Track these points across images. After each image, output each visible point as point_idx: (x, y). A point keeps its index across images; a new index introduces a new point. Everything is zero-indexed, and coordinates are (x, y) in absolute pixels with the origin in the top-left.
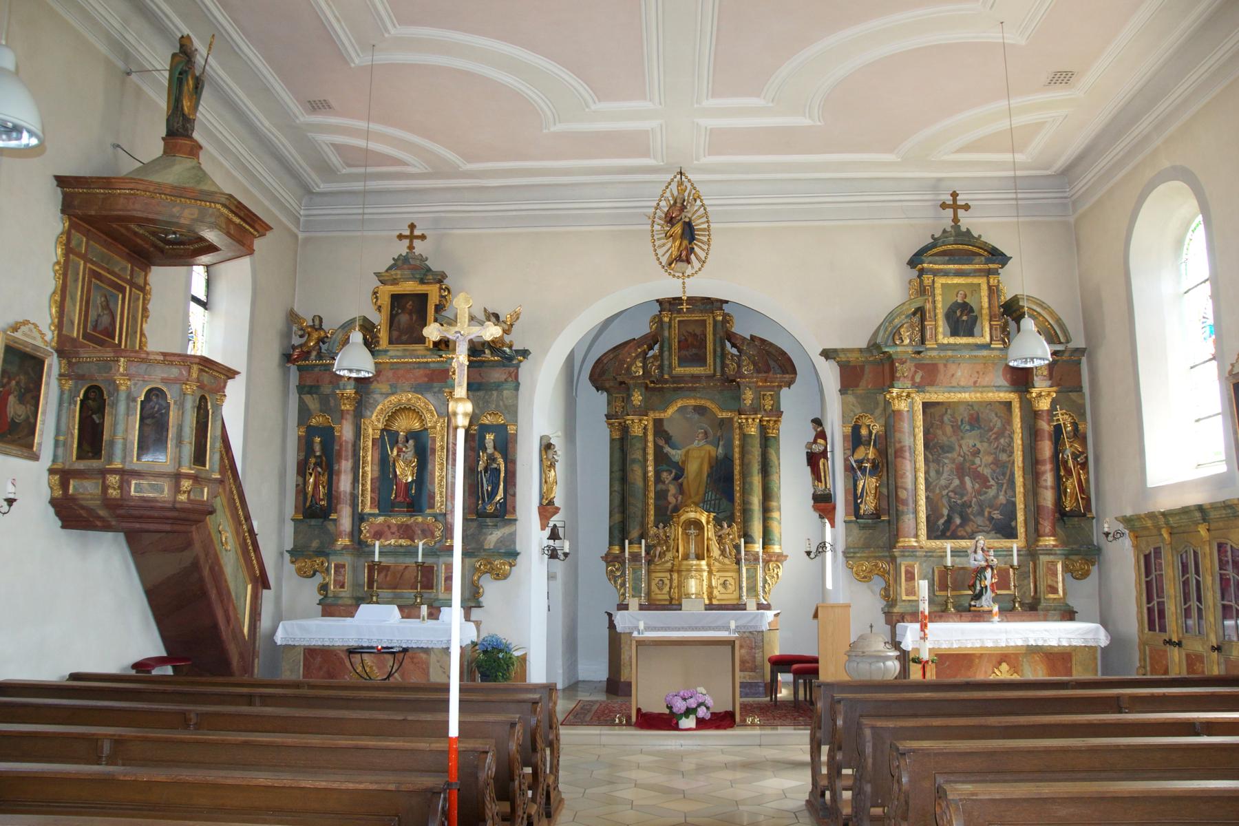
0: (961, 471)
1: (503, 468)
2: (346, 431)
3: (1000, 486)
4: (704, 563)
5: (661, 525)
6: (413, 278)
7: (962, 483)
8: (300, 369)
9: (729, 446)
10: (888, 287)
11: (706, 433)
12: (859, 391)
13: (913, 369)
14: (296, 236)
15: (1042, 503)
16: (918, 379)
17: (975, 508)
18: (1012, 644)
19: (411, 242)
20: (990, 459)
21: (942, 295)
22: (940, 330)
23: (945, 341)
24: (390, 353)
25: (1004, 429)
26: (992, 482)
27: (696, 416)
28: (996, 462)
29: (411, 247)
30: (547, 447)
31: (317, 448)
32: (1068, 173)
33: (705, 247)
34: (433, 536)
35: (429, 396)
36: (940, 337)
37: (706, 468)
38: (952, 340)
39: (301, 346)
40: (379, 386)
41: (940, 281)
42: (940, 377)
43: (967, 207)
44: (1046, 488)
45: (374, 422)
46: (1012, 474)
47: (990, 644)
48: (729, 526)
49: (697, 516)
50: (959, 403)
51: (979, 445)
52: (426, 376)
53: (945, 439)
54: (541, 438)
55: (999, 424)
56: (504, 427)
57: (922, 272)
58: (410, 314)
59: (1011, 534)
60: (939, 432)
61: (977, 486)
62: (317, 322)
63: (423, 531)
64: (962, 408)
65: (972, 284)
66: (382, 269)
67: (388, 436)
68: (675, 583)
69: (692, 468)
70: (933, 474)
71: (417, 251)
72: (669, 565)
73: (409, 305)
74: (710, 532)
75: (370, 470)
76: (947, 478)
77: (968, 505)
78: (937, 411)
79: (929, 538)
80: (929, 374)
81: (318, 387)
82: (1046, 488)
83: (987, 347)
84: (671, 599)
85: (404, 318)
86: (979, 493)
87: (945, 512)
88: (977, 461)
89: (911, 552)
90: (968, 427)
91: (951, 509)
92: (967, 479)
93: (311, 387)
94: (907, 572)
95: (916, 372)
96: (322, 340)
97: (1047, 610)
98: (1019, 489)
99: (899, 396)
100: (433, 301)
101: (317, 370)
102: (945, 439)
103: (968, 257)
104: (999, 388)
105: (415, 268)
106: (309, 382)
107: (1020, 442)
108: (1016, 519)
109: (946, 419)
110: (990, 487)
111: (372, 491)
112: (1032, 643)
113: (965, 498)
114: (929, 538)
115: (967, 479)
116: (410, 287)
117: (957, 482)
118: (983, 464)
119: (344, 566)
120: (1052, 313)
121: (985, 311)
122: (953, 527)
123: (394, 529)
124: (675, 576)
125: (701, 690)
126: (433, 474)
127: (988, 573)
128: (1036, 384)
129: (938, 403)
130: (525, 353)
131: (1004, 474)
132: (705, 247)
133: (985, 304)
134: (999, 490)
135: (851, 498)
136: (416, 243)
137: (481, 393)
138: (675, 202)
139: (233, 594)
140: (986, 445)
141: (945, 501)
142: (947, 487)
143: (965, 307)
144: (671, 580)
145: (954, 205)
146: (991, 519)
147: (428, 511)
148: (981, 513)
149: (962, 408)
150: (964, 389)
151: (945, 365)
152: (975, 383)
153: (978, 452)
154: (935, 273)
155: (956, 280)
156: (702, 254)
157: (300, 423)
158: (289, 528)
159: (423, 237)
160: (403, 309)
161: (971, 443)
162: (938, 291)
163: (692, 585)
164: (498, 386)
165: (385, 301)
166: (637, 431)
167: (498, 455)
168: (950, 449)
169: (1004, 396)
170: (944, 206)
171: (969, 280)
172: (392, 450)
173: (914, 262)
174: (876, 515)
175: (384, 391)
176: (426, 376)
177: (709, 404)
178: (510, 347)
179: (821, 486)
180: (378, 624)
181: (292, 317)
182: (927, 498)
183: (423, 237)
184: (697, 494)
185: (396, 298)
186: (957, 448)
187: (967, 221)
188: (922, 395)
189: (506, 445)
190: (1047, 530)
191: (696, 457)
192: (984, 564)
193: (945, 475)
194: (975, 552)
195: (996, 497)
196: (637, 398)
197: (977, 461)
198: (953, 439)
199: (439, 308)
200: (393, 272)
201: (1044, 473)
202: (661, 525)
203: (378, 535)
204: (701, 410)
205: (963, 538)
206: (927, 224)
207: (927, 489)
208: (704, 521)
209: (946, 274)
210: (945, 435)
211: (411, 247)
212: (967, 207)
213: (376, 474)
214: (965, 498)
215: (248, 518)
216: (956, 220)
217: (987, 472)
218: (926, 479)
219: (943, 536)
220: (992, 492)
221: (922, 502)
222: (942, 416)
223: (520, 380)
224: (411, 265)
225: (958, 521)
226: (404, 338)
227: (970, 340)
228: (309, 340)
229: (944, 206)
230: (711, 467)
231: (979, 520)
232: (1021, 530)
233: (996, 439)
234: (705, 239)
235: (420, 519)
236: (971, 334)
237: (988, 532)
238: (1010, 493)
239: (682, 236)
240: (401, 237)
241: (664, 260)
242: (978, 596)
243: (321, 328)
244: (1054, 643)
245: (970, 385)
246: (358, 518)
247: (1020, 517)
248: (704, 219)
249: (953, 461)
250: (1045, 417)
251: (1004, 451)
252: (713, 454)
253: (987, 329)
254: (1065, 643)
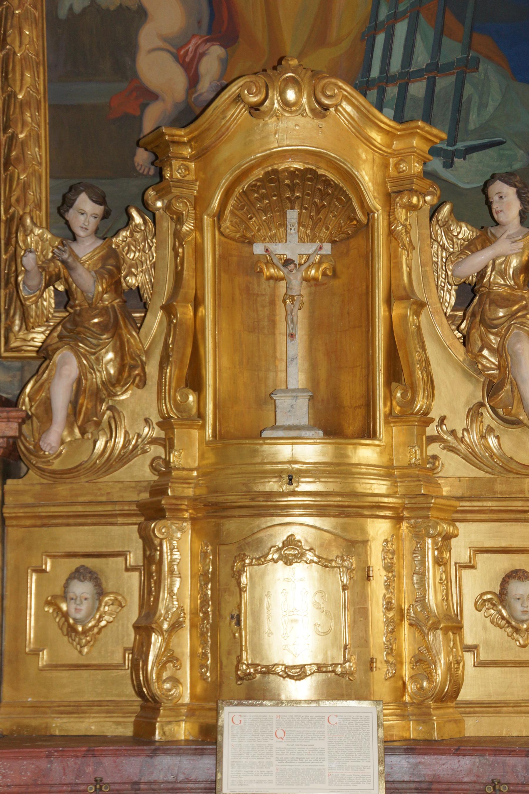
4: (366, 454)
5: (86, 211)
68: (179, 592)
72: (141, 470)
84: (150, 706)
124: (179, 546)
144: (151, 566)
163: (293, 611)
184: (319, 37)
202: (86, 211)
208: (367, 176)
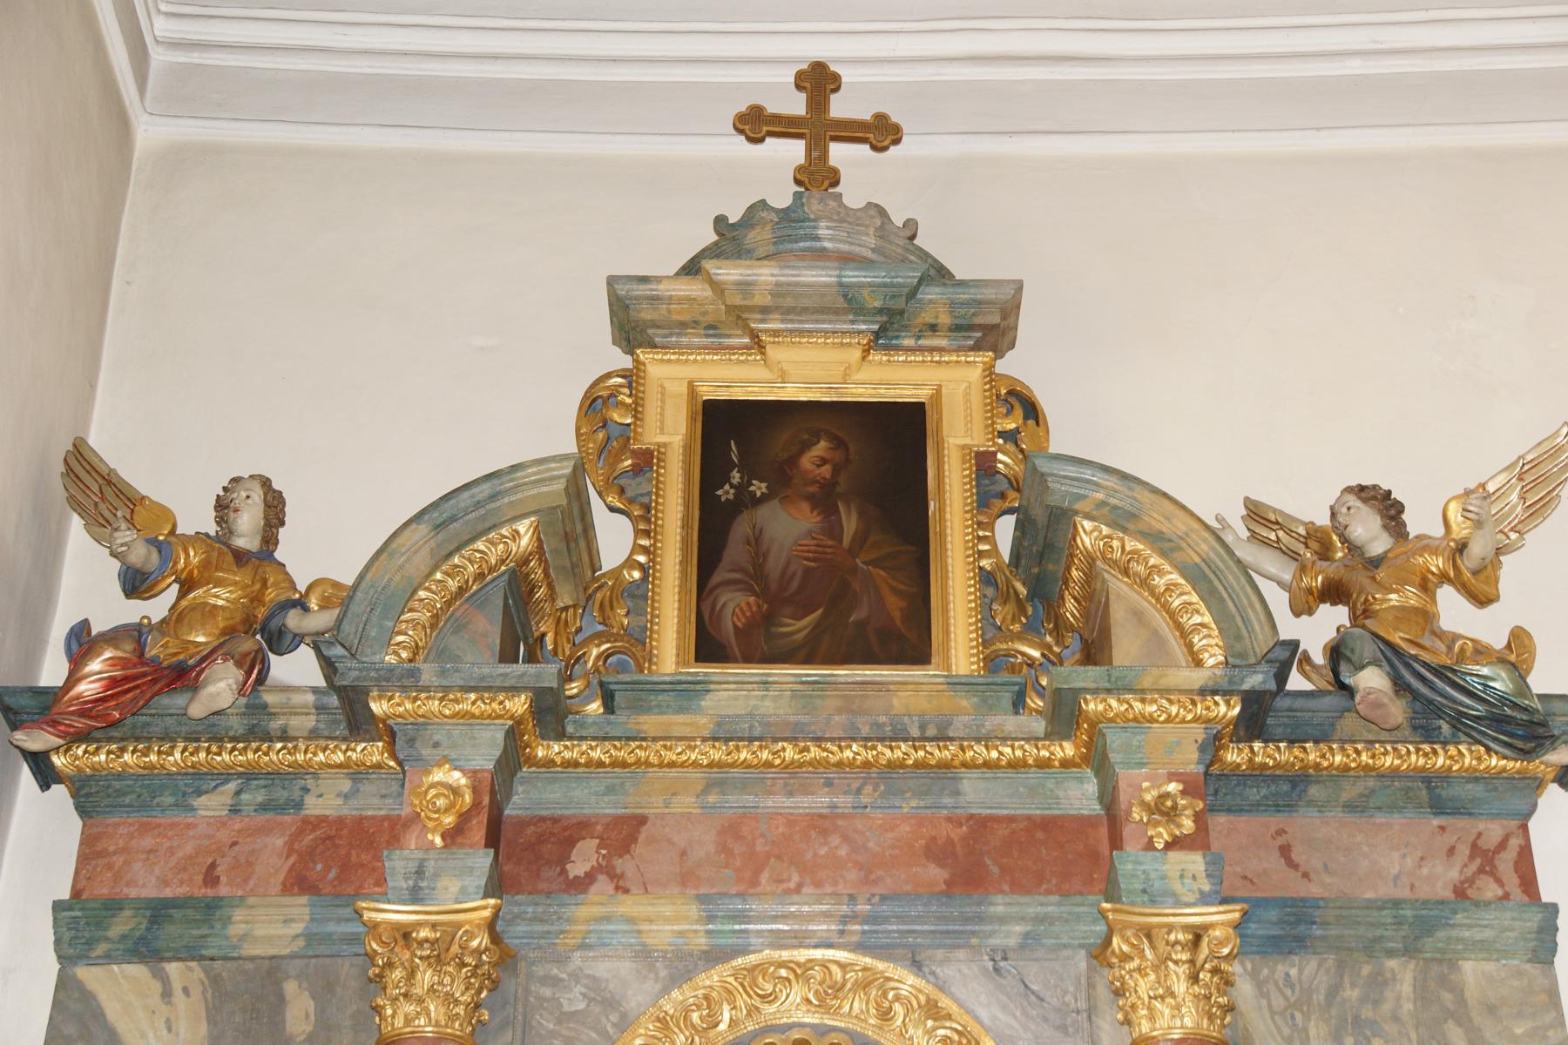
6: (850, 303)
8: (91, 796)
29: (817, 177)
39: (136, 633)
40: (628, 906)
52: (937, 852)
58: (825, 500)
71: (853, 193)
73: (815, 458)
81: (211, 910)
85: (786, 527)
93: (159, 911)
100: (959, 433)
101: (212, 805)
106: (146, 884)
116: (813, 369)
137: (1307, 969)
159: (880, 133)
160: (783, 479)
164: (1419, 927)
165: (670, 431)
175: (662, 934)
176: (937, 852)
183: (880, 133)
200: (728, 272)
211: (817, 177)
226: (797, 627)
240: (756, 124)
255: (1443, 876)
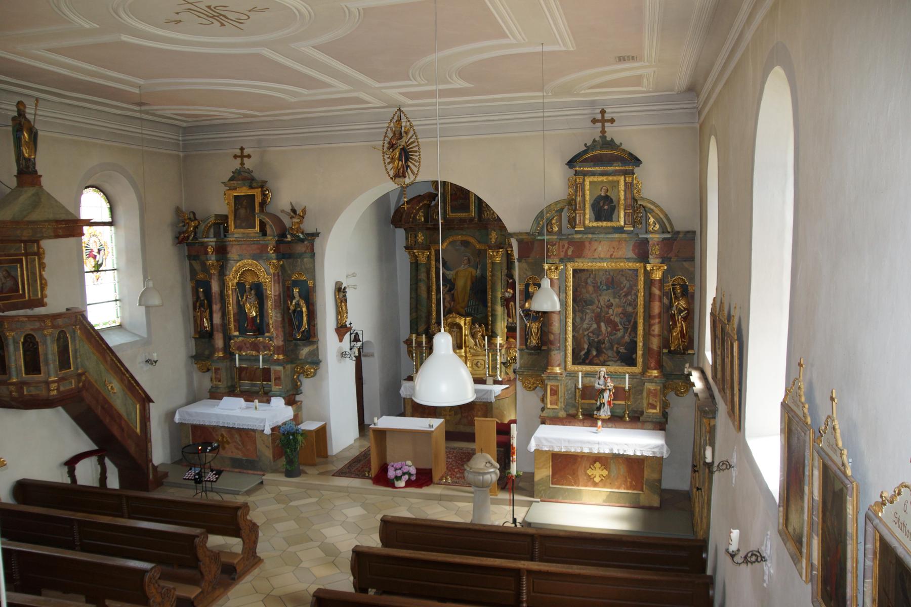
0: (598, 318)
1: (304, 310)
2: (215, 287)
3: (626, 329)
7: (599, 327)
8: (188, 245)
9: (484, 269)
10: (554, 182)
11: (469, 260)
12: (530, 260)
13: (566, 245)
14: (179, 156)
15: (651, 346)
16: (570, 253)
17: (607, 345)
18: (602, 451)
19: (242, 160)
20: (620, 310)
21: (590, 190)
22: (587, 216)
23: (591, 225)
24: (236, 236)
25: (631, 288)
26: (620, 327)
27: (463, 248)
28: (625, 314)
29: (242, 164)
30: (340, 290)
31: (201, 295)
32: (692, 89)
33: (417, 164)
34: (270, 350)
35: (261, 262)
36: (587, 222)
37: (469, 283)
38: (595, 224)
41: (588, 180)
42: (587, 252)
43: (612, 121)
44: (654, 336)
45: (232, 280)
46: (636, 323)
47: (586, 450)
48: (480, 326)
49: (458, 320)
50: (599, 270)
51: (612, 300)
53: (588, 296)
54: (337, 283)
55: (628, 285)
56: (306, 281)
57: (576, 173)
58: (246, 208)
59: (632, 362)
60: (584, 291)
61: (609, 329)
62: (192, 216)
63: (264, 347)
64: (601, 273)
65: (613, 182)
66: (226, 179)
67: (240, 286)
69: (460, 283)
70: (578, 320)
71: (246, 166)
74: (466, 331)
75: (232, 308)
76: (588, 323)
77: (600, 342)
78: (584, 276)
79: (574, 363)
80: (579, 249)
82: (654, 336)
83: (620, 230)
86: (611, 334)
87: (586, 347)
88: (611, 311)
89: (555, 377)
90: (605, 287)
91: (590, 345)
92: (602, 324)
94: (551, 390)
95: (568, 248)
96: (196, 227)
97: (644, 422)
98: (640, 332)
99: (550, 269)
100: (258, 200)
102: (588, 296)
103: (610, 160)
104: (628, 260)
105: (244, 179)
107: (642, 299)
108: (636, 353)
109: (589, 281)
110: (619, 330)
111: (235, 321)
112: (615, 451)
113: (600, 338)
114: (574, 363)
115: (602, 324)
116: (244, 191)
117: (595, 326)
118: (615, 314)
119: (219, 369)
120: (661, 210)
121: (622, 202)
122: (590, 357)
123: (248, 345)
125: (409, 463)
126: (267, 311)
127: (606, 395)
128: (651, 261)
129: (584, 270)
130: (316, 234)
131: (629, 321)
132: (417, 164)
133: (622, 197)
134: (625, 332)
135: (523, 334)
136: (246, 160)
138: (395, 134)
139: (124, 414)
140: (617, 300)
141: (586, 339)
142: (588, 329)
143: (607, 199)
145: (603, 119)
146: (618, 352)
147: (267, 334)
148: (611, 348)
149: (601, 273)
150: (602, 260)
151: (590, 243)
152: (611, 255)
153: (612, 305)
154: (585, 174)
155: (600, 179)
156: (415, 169)
157: (191, 279)
158: (193, 341)
159: (249, 156)
161: (607, 298)
162: (587, 187)
164: (301, 256)
166: (423, 259)
167: (302, 303)
168: (592, 303)
169: (631, 265)
170: (594, 121)
171: (610, 178)
172: (242, 298)
173: (571, 163)
174: (538, 348)
177: (472, 240)
178: (302, 233)
179: (510, 320)
180: (232, 411)
181: (178, 211)
182: (573, 336)
185: (236, 197)
186: (596, 302)
187: (612, 132)
188: (572, 264)
189: (309, 296)
190: (652, 365)
191: (464, 276)
192: (603, 387)
193: (587, 321)
194: (599, 378)
195: (623, 337)
196: (421, 238)
197: (611, 311)
198: (594, 296)
199: (263, 204)
201: (653, 325)
203: (240, 349)
204: (465, 244)
205: (597, 364)
206: (582, 135)
207: (573, 330)
208: (462, 324)
209: (593, 174)
210: (589, 292)
211: (242, 164)
212: (612, 121)
213: (236, 311)
214: (600, 338)
215: (127, 371)
216: (603, 132)
217: (617, 320)
218: (573, 324)
219: (583, 362)
220: (620, 334)
221: (570, 339)
222: (587, 279)
223: (317, 249)
224: (242, 177)
225: (594, 353)
226: (244, 225)
227: (609, 224)
228: (189, 228)
229: (594, 121)
230: (473, 283)
231: (610, 353)
232: (640, 360)
233: (626, 296)
234: (417, 158)
235: (261, 339)
236: (611, 220)
237: (615, 362)
238: (633, 335)
239: (400, 159)
240: (236, 157)
241: (392, 173)
242: (599, 409)
243: (195, 219)
244: (630, 453)
245: (607, 256)
246: (227, 338)
247: (640, 352)
248: (416, 144)
249: (593, 311)
250: (657, 285)
251: (630, 305)
252: (474, 274)
253: (622, 215)
254: (638, 454)
255: (304, 249)
